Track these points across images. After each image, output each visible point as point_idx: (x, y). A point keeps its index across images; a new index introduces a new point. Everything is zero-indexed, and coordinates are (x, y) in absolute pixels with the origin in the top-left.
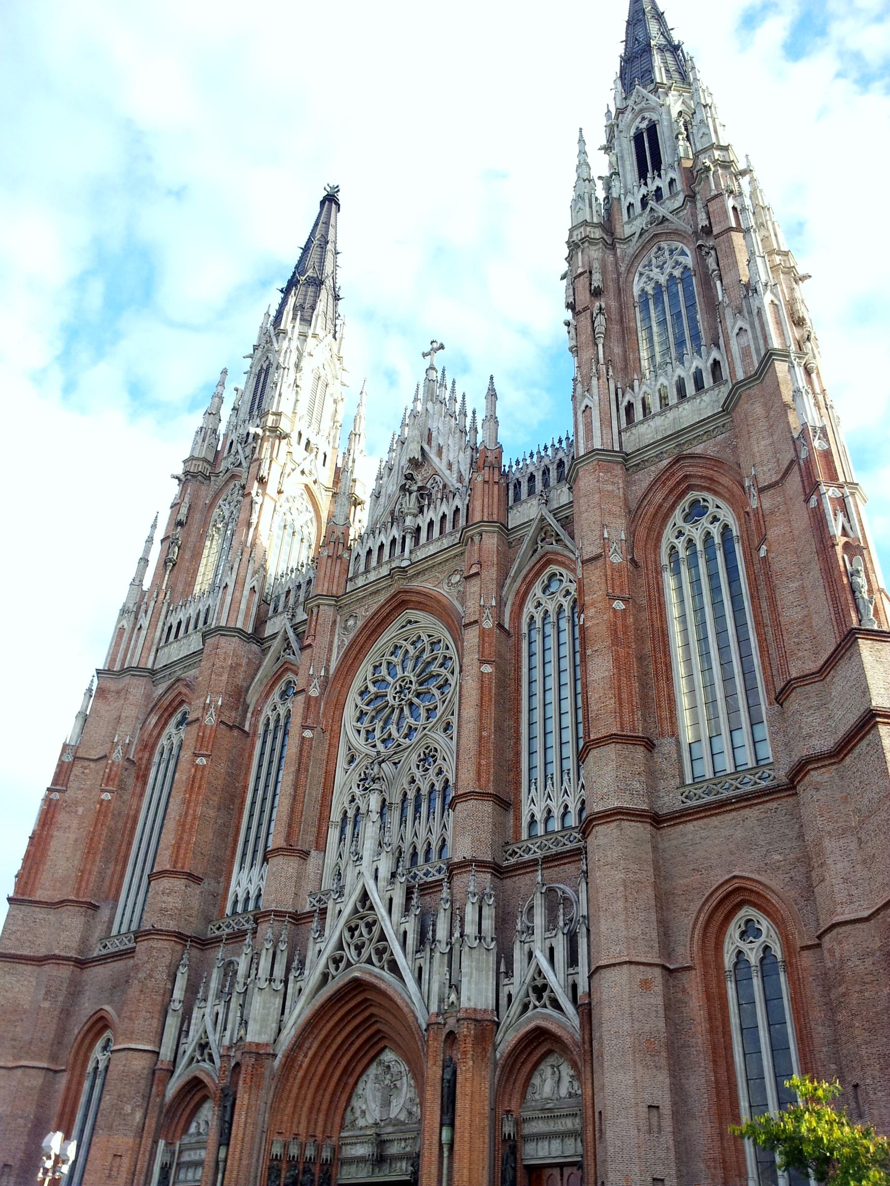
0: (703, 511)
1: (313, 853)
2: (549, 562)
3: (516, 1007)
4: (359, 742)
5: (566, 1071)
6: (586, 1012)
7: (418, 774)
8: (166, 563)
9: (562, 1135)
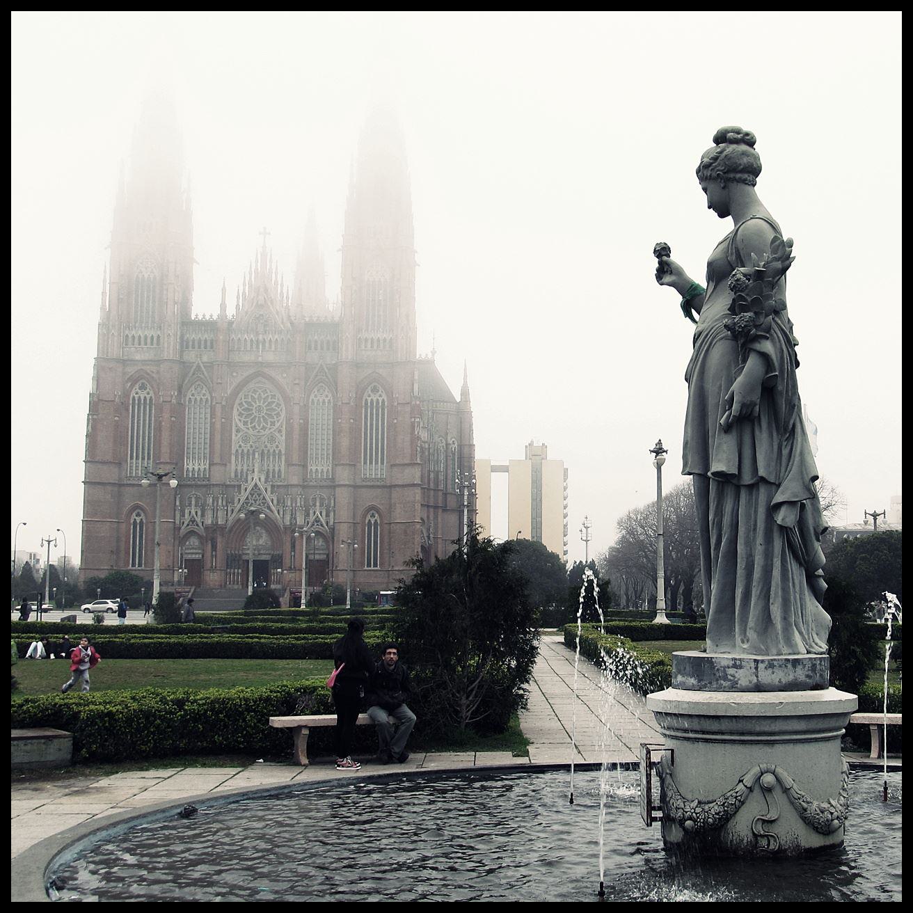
0: (378, 391)
1: (228, 464)
2: (321, 382)
4: (241, 425)
5: (321, 540)
6: (333, 530)
7: (269, 445)
8: (118, 299)
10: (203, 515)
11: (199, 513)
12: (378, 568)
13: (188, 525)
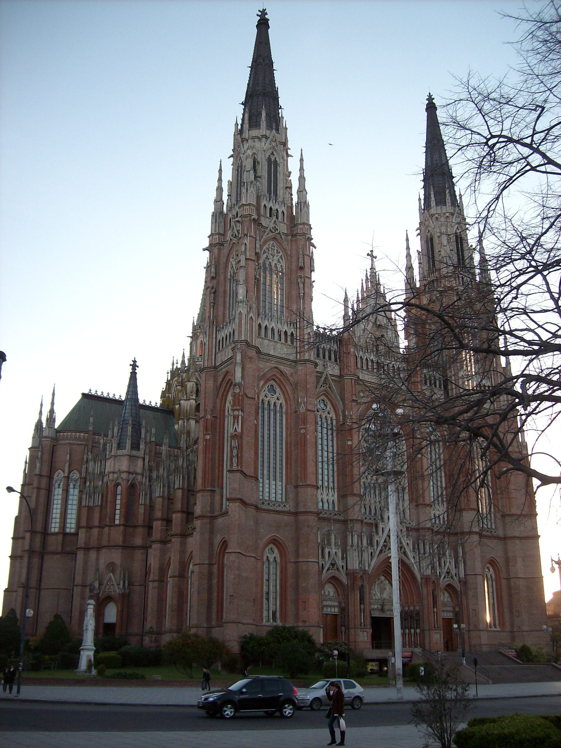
3: (443, 577)
5: (447, 595)
6: (464, 582)
9: (446, 611)
10: (344, 558)
11: (340, 554)
12: (498, 629)
13: (328, 570)
